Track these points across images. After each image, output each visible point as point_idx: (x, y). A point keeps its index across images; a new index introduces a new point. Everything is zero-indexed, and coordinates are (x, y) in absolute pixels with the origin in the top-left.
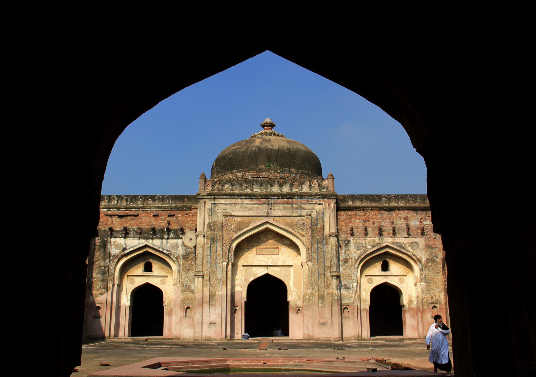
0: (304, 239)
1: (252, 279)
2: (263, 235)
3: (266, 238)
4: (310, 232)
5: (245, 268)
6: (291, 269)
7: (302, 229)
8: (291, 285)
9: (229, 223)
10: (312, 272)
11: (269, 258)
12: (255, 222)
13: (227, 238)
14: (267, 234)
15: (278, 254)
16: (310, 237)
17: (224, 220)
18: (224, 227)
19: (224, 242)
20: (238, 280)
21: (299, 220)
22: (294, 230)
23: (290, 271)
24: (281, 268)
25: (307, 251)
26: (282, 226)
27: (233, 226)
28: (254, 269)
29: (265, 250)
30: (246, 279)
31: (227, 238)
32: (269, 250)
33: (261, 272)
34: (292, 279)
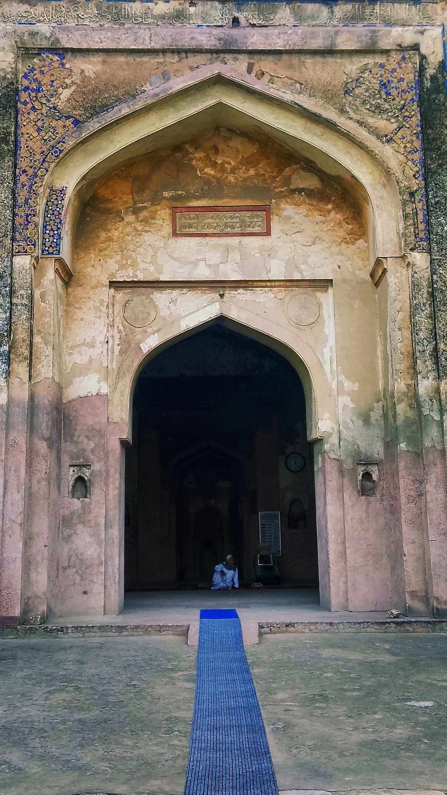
0: (388, 152)
1: (151, 343)
2: (200, 155)
3: (214, 165)
4: (416, 120)
5: (121, 296)
6: (327, 299)
7: (378, 110)
8: (327, 367)
9: (46, 80)
10: (432, 295)
11: (227, 250)
12: (166, 77)
13: (36, 146)
14: (216, 150)
15: (268, 233)
16: (417, 144)
17: (22, 68)
18: (24, 96)
19: (23, 164)
20: (92, 345)
21: (365, 69)
22: (342, 111)
23: (320, 306)
24: (281, 293)
25: (404, 203)
26: (288, 97)
27: (65, 94)
28: (161, 298)
29: (209, 219)
30: (127, 345)
31: (36, 146)
32: (227, 218)
33: (193, 312)
34: (332, 342)
